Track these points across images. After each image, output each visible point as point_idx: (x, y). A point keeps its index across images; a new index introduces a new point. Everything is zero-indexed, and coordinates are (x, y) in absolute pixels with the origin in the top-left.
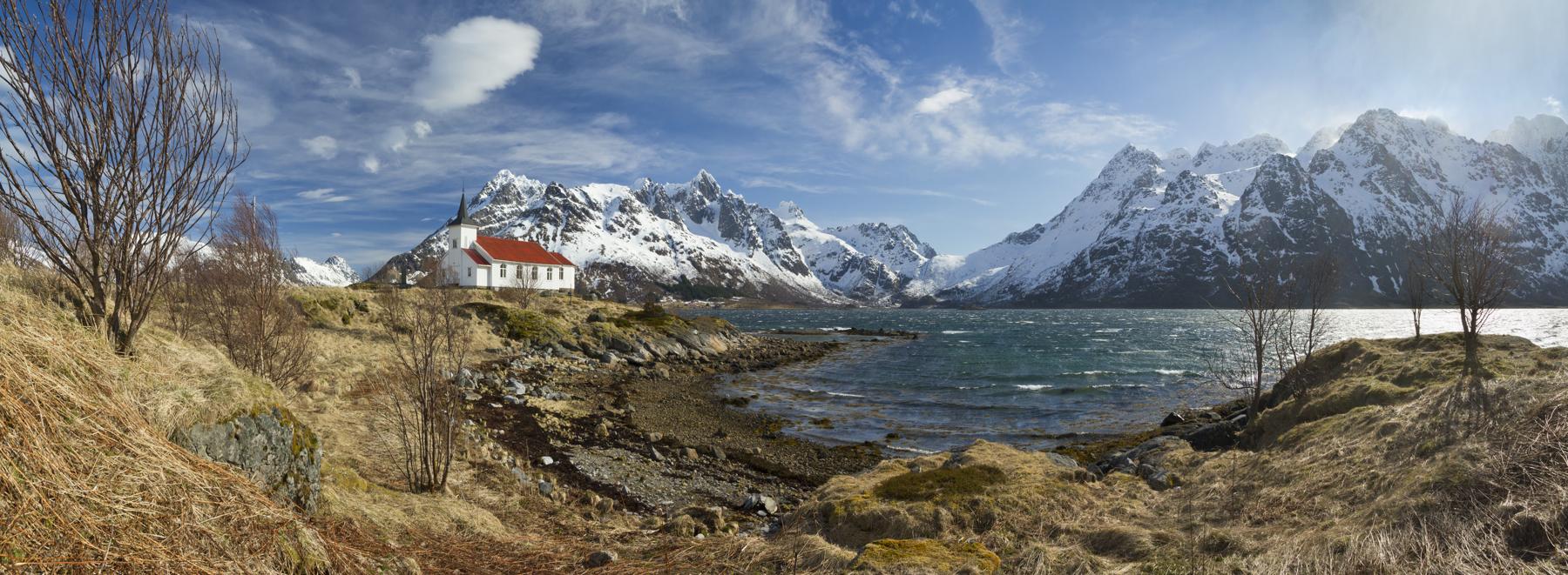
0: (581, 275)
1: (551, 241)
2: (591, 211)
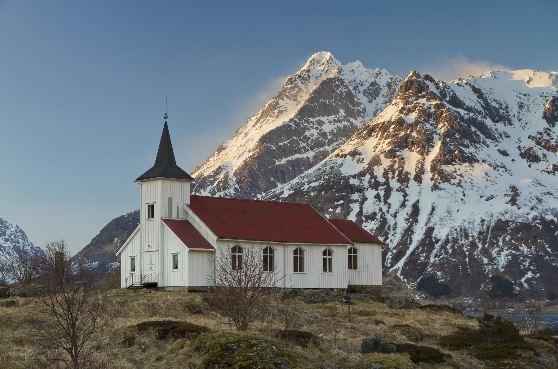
0: (473, 245)
1: (412, 183)
2: (489, 122)
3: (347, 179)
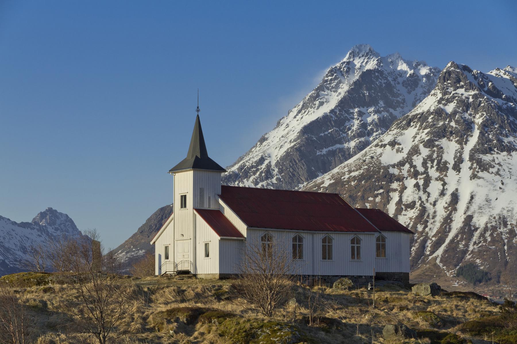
1: (451, 172)
3: (387, 168)
